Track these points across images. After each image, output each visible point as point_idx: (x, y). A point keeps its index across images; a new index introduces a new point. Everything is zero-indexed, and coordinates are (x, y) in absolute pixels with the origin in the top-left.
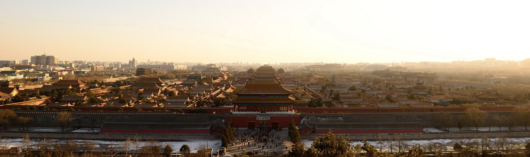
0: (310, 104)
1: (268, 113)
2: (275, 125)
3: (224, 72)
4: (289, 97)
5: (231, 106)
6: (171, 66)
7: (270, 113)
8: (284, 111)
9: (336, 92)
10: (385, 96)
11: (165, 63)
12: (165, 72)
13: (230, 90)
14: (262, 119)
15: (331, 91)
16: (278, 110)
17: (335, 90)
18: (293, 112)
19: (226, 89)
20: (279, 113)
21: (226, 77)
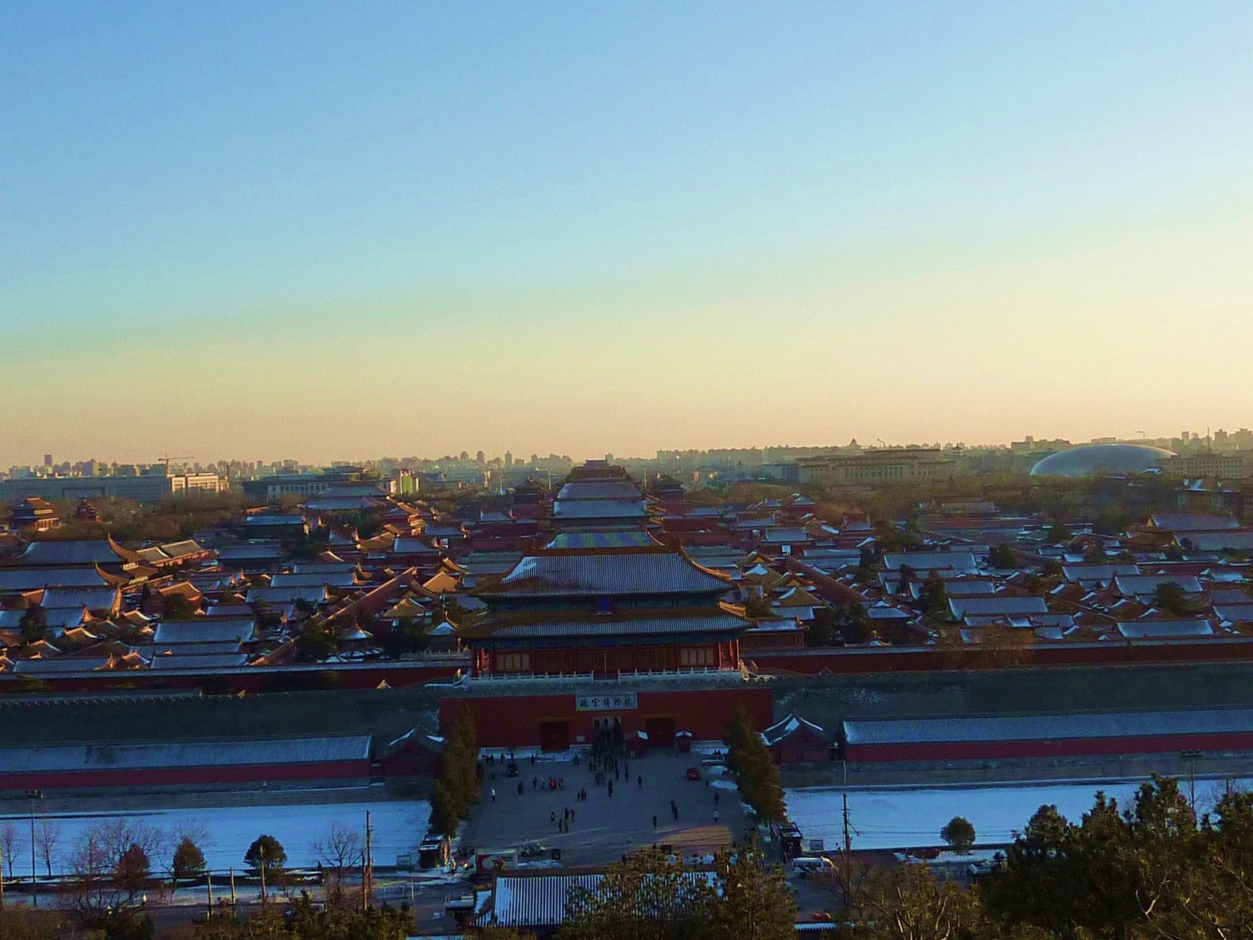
0: (813, 633)
1: (629, 678)
2: (665, 727)
3: (406, 498)
4: (722, 605)
5: (459, 655)
6: (155, 478)
7: (637, 676)
8: (699, 667)
9: (923, 575)
10: (1151, 586)
11: (127, 469)
12: (132, 511)
13: (439, 582)
14: (601, 706)
15: (907, 574)
16: (674, 666)
17: (922, 563)
18: (743, 673)
19: (422, 579)
20: (679, 675)
21: (416, 525)
